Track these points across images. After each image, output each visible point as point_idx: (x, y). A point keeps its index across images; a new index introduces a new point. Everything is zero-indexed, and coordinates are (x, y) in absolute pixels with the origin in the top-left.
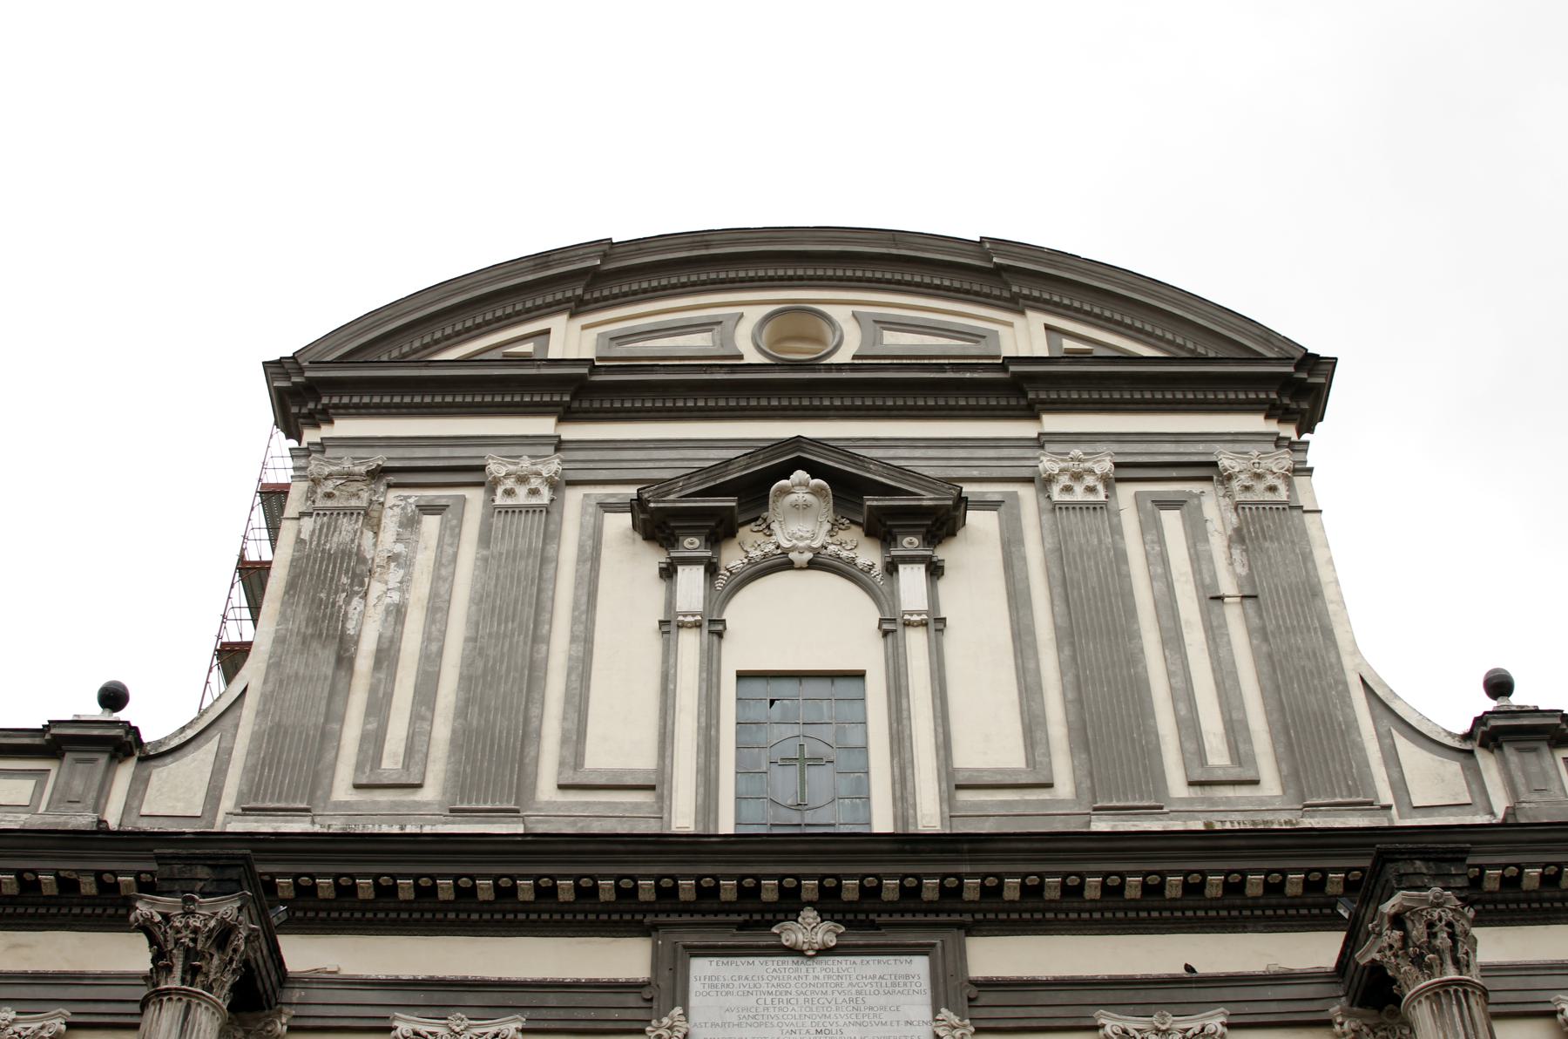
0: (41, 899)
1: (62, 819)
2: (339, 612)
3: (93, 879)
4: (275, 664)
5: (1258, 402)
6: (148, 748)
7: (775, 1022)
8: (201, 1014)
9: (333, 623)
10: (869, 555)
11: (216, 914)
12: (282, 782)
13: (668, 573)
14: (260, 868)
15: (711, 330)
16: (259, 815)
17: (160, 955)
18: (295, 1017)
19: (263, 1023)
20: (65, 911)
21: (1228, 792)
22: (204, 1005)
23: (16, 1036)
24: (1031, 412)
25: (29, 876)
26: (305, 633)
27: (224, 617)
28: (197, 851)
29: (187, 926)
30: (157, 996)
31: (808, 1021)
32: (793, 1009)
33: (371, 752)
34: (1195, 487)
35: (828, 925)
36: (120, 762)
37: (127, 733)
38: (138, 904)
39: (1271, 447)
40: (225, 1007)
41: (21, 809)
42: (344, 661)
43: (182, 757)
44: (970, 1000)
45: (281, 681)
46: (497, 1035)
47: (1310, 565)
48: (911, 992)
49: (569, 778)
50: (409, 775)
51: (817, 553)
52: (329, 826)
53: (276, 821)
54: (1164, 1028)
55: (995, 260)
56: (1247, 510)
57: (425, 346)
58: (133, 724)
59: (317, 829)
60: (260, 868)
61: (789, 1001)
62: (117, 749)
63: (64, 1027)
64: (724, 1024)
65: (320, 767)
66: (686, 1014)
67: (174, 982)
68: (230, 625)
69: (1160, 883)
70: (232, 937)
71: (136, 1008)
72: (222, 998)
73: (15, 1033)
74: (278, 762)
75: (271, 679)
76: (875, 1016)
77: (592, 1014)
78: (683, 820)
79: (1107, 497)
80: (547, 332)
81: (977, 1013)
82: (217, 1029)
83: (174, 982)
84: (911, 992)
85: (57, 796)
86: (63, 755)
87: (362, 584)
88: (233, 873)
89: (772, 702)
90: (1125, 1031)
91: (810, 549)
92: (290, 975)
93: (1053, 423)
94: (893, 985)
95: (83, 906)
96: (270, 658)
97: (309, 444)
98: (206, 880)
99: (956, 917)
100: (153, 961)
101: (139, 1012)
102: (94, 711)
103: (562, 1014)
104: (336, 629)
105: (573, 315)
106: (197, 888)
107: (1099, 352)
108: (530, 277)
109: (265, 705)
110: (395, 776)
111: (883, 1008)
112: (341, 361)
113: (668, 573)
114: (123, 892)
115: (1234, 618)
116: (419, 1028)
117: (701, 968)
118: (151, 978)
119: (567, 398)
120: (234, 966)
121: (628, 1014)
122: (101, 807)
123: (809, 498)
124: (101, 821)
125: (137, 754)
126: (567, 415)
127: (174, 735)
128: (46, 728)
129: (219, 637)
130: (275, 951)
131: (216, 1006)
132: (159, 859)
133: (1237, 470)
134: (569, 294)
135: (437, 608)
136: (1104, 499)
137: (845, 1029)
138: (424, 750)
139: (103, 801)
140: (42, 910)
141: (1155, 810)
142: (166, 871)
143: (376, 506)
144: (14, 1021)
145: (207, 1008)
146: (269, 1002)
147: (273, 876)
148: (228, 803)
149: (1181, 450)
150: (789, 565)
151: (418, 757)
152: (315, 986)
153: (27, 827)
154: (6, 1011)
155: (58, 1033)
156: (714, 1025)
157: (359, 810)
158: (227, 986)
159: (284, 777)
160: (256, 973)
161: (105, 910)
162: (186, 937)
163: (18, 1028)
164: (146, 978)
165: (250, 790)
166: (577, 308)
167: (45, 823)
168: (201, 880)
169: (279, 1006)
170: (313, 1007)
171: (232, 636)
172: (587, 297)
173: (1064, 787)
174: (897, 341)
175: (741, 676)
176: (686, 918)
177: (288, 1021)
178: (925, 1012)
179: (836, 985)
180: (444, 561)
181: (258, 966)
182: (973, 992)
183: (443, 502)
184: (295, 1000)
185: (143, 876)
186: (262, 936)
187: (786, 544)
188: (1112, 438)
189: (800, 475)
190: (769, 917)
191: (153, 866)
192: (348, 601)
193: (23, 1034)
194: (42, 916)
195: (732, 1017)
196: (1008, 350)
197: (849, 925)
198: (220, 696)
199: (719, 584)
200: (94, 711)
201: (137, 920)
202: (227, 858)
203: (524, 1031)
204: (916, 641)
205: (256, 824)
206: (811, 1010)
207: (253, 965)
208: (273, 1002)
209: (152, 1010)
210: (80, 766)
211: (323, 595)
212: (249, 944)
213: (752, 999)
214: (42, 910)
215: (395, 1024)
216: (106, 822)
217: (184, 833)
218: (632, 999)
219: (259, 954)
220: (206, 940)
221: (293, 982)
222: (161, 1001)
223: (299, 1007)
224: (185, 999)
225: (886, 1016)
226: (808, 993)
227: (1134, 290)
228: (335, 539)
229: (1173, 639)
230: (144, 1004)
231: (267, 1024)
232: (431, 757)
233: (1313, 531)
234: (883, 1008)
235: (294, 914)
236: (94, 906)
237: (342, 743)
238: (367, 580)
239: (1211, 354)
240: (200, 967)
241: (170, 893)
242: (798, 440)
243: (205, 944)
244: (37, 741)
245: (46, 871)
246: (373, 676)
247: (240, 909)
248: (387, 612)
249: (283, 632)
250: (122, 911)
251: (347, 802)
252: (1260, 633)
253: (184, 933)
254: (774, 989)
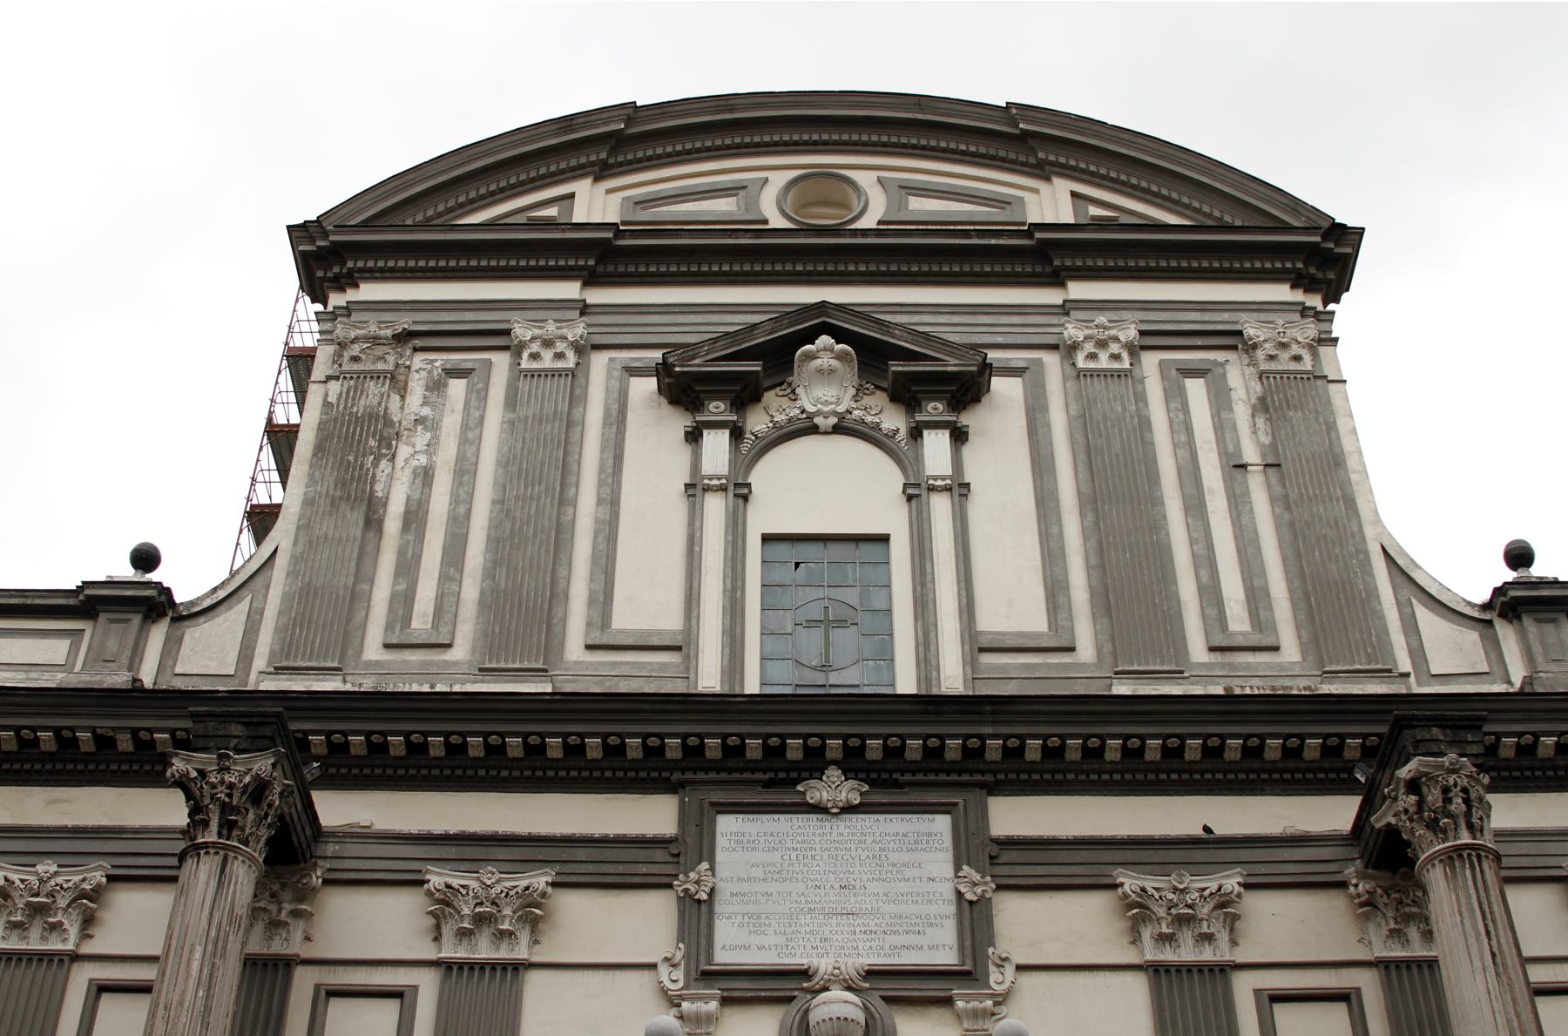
0: (79, 756)
1: (98, 678)
2: (367, 474)
3: (129, 736)
4: (304, 526)
5: (1285, 271)
6: (181, 608)
7: (800, 877)
8: (238, 867)
9: (361, 486)
10: (893, 420)
11: (250, 770)
12: (313, 642)
13: (693, 437)
14: (293, 726)
15: (735, 195)
16: (291, 674)
17: (196, 810)
18: (330, 870)
19: (298, 876)
20: (102, 767)
21: (1249, 658)
22: (240, 858)
23: (58, 888)
24: (1056, 279)
25: (66, 734)
26: (333, 496)
27: (253, 479)
28: (231, 709)
29: (222, 782)
30: (195, 850)
31: (832, 877)
32: (818, 865)
33: (400, 613)
34: (1220, 356)
35: (852, 783)
36: (153, 622)
37: (160, 594)
38: (174, 761)
39: (1297, 316)
40: (261, 860)
41: (57, 668)
42: (373, 523)
43: (214, 618)
44: (991, 857)
45: (311, 543)
46: (527, 888)
47: (1333, 435)
48: (933, 850)
49: (597, 638)
50: (438, 635)
51: (841, 417)
52: (360, 685)
53: (308, 680)
54: (1181, 887)
55: (1021, 126)
56: (1271, 379)
57: (450, 210)
58: (165, 585)
59: (348, 687)
60: (293, 726)
61: (813, 857)
62: (151, 610)
63: (104, 880)
64: (749, 879)
65: (351, 626)
66: (712, 869)
67: (211, 836)
68: (260, 488)
69: (1259, 745)
70: (267, 793)
71: (174, 861)
72: (258, 852)
73: (57, 885)
74: (309, 623)
75: (301, 541)
76: (898, 872)
77: (621, 869)
78: (709, 679)
79: (1131, 364)
80: (572, 196)
81: (998, 870)
82: (254, 881)
83: (211, 836)
84: (933, 850)
85: (92, 655)
86: (98, 616)
87: (389, 447)
88: (267, 731)
89: (797, 565)
90: (1143, 890)
91: (835, 413)
92: (324, 830)
93: (1078, 290)
94: (916, 842)
95: (120, 763)
96: (300, 519)
97: (334, 308)
98: (240, 737)
99: (978, 777)
100: (189, 815)
101: (177, 864)
102: (127, 572)
103: (591, 868)
104: (364, 491)
105: (597, 179)
106: (232, 745)
107: (1125, 219)
108: (554, 141)
109: (295, 564)
110: (424, 636)
111: (906, 865)
112: (366, 225)
113: (693, 437)
114: (159, 749)
115: (1258, 489)
116: (450, 881)
117: (727, 824)
118: (189, 831)
119: (591, 262)
120: (269, 820)
121: (656, 869)
122: (136, 665)
123: (834, 362)
124: (135, 680)
125: (170, 614)
126: (592, 279)
127: (206, 596)
128: (80, 589)
129: (248, 499)
130: (309, 806)
131: (252, 859)
132: (195, 717)
133: (1262, 339)
134: (593, 158)
135: (465, 471)
136: (1128, 366)
137: (868, 885)
138: (453, 610)
139: (137, 660)
140: (80, 767)
141: (1175, 675)
142: (200, 728)
143: (402, 370)
144: (56, 874)
145: (243, 862)
146: (304, 855)
147: (306, 733)
148: (260, 662)
149: (1207, 319)
150: (814, 430)
151: (447, 617)
152: (348, 840)
153: (63, 686)
154: (47, 864)
155: (99, 885)
156: (740, 880)
157: (389, 669)
158: (263, 841)
159: (315, 635)
160: (291, 827)
161: (142, 767)
162: (222, 792)
163: (59, 880)
164: (183, 832)
165: (282, 650)
166: (601, 172)
167: (80, 682)
168: (235, 737)
169: (313, 860)
170: (347, 860)
171: (262, 498)
172: (611, 161)
173: (1086, 651)
174: (922, 206)
175: (767, 539)
176: (712, 776)
177: (323, 873)
178: (948, 870)
179: (860, 842)
180: (471, 424)
181: (292, 820)
182: (995, 850)
183: (469, 365)
184: (329, 854)
185: (178, 733)
186: (296, 791)
187: (811, 409)
188: (1138, 306)
189: (825, 340)
190: (794, 775)
191: (188, 724)
192: (376, 464)
193: (65, 886)
194: (81, 772)
195: (759, 873)
196: (1033, 218)
197: (872, 783)
198: (251, 557)
199: (744, 448)
200: (127, 572)
201: (173, 776)
202: (261, 716)
203: (554, 885)
204: (940, 507)
205: (288, 683)
206: (835, 865)
207: (288, 820)
208: (308, 856)
209: (190, 864)
210: (114, 626)
211: (351, 458)
212: (283, 800)
213: (777, 855)
214: (80, 767)
215: (428, 877)
216: (141, 680)
217: (218, 692)
218: (659, 855)
219: (293, 809)
220: (242, 795)
221: (328, 837)
222: (199, 854)
223: (334, 860)
224: (222, 853)
225: (909, 873)
226: (833, 849)
227: (1160, 157)
228: (362, 402)
229: (1195, 506)
230: (182, 857)
231: (302, 877)
232: (460, 617)
233: (1337, 401)
234: (906, 865)
235: (327, 770)
236: (131, 763)
237: (372, 603)
238: (394, 443)
239: (1238, 223)
240: (236, 821)
241: (205, 750)
242: (823, 306)
243: (241, 798)
244: (72, 601)
245: (84, 729)
246: (401, 538)
247: (274, 765)
248: (415, 474)
249: (312, 494)
250: (158, 768)
251: (376, 661)
252: (1282, 502)
253: (220, 789)
254: (799, 846)
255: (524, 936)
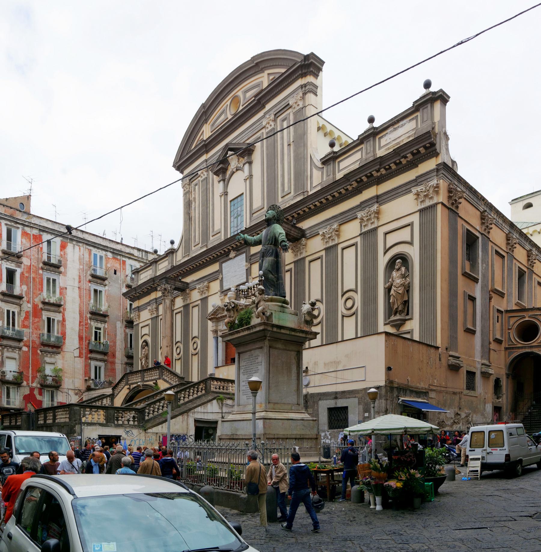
5: (298, 76)
51: (237, 167)
57: (189, 149)
105: (206, 123)
112: (180, 160)
242: (227, 145)
255: (207, 292)
